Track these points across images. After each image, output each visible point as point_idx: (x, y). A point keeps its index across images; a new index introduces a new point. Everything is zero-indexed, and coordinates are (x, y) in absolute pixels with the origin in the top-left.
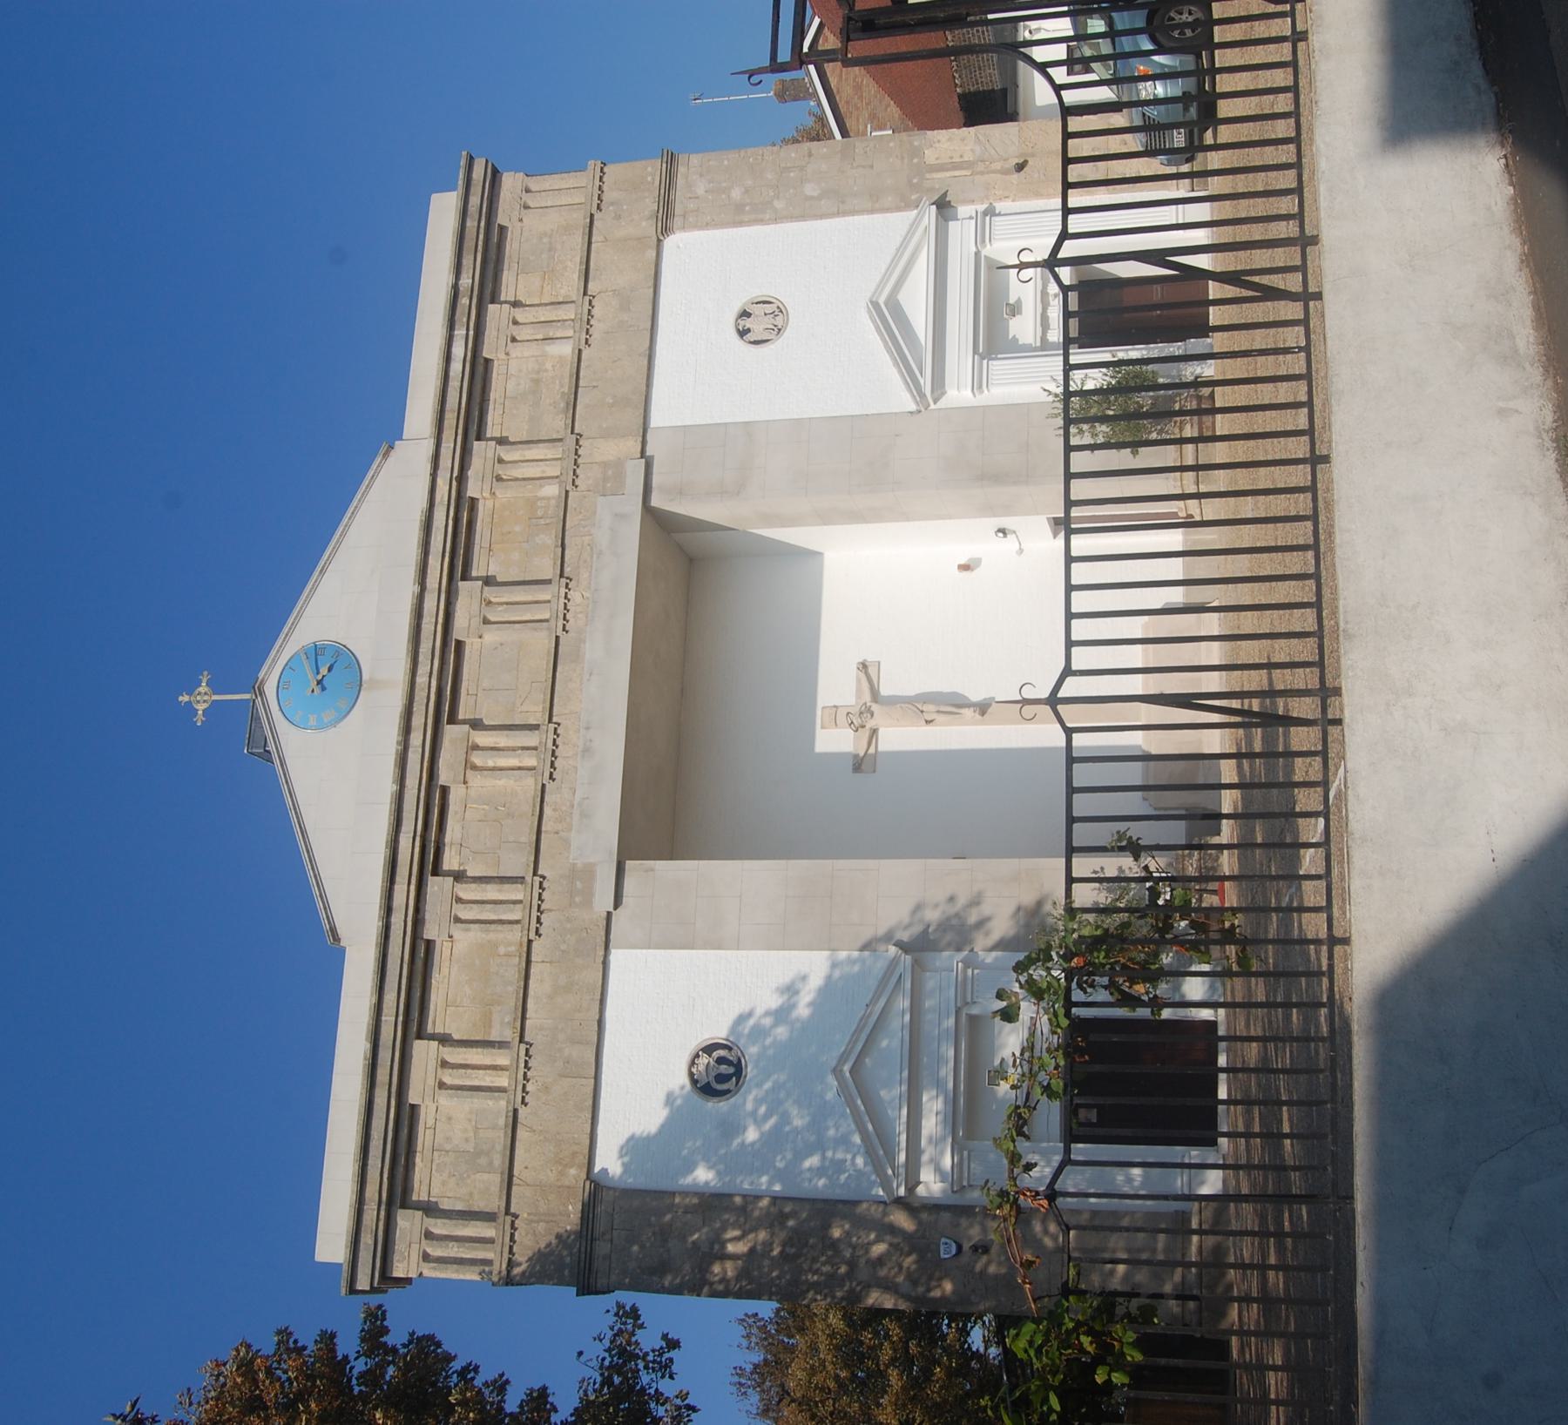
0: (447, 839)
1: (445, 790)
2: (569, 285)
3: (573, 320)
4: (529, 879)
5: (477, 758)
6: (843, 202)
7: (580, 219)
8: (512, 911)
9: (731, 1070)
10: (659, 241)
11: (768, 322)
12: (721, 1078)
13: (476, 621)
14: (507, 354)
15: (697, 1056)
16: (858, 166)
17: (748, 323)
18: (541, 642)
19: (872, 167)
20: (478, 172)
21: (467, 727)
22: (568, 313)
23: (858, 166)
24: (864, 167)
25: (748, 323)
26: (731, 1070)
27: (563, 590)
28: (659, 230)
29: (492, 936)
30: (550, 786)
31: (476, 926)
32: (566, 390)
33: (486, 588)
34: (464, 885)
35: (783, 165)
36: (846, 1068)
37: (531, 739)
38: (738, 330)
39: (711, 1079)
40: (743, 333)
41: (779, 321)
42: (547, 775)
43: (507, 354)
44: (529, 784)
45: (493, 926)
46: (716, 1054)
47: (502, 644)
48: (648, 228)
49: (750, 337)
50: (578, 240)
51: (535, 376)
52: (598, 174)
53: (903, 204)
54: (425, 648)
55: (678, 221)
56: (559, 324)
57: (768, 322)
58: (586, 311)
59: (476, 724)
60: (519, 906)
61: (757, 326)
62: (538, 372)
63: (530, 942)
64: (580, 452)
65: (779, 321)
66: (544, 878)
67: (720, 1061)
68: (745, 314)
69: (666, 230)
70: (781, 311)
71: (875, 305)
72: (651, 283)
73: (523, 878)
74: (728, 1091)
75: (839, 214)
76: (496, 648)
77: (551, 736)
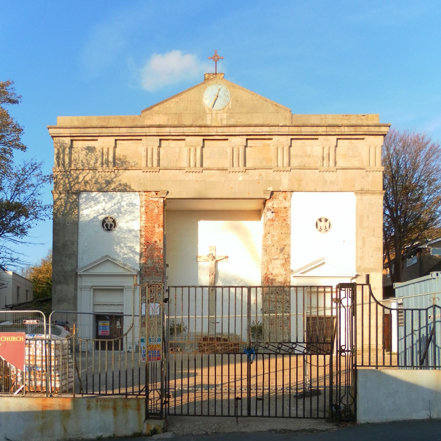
0: (170, 141)
1: (184, 140)
2: (341, 163)
3: (329, 166)
4: (158, 168)
5: (192, 149)
6: (361, 248)
7: (365, 164)
8: (150, 163)
9: (109, 228)
10: (353, 191)
11: (323, 227)
12: (107, 225)
13: (233, 145)
14: (319, 146)
15: (112, 219)
16: (372, 253)
17: (323, 220)
18: (227, 164)
19: (372, 257)
20: (384, 130)
21: (202, 145)
22: (332, 163)
23: (372, 253)
24: (372, 254)
25: (323, 220)
26: (109, 228)
27: (242, 171)
28: (356, 192)
29: (143, 158)
30: (184, 171)
31: (146, 154)
32: (306, 165)
33: (244, 147)
34: (157, 149)
35: (375, 229)
36: (108, 258)
37: (198, 165)
38: (321, 218)
39: (107, 223)
40: (320, 220)
41: (323, 230)
42: (187, 170)
43: (319, 146)
44: (184, 164)
45: (145, 159)
46: (113, 224)
47: (227, 153)
48: (358, 188)
49: (319, 222)
50: (358, 165)
51: (311, 156)
52: (379, 170)
53: (358, 267)
54: (226, 129)
55: (359, 196)
56: (328, 162)
57: (323, 227)
58: (331, 170)
59: (203, 147)
60: (151, 166)
61: (322, 224)
62: (313, 156)
63: (141, 169)
64: (285, 172)
65: (323, 230)
66: (159, 171)
67: (111, 225)
68: (326, 220)
69: (356, 193)
70: (326, 231)
71: (324, 259)
72: (339, 190)
73: (159, 166)
74: (104, 227)
75: (357, 247)
76: (226, 151)
77: (198, 171)
